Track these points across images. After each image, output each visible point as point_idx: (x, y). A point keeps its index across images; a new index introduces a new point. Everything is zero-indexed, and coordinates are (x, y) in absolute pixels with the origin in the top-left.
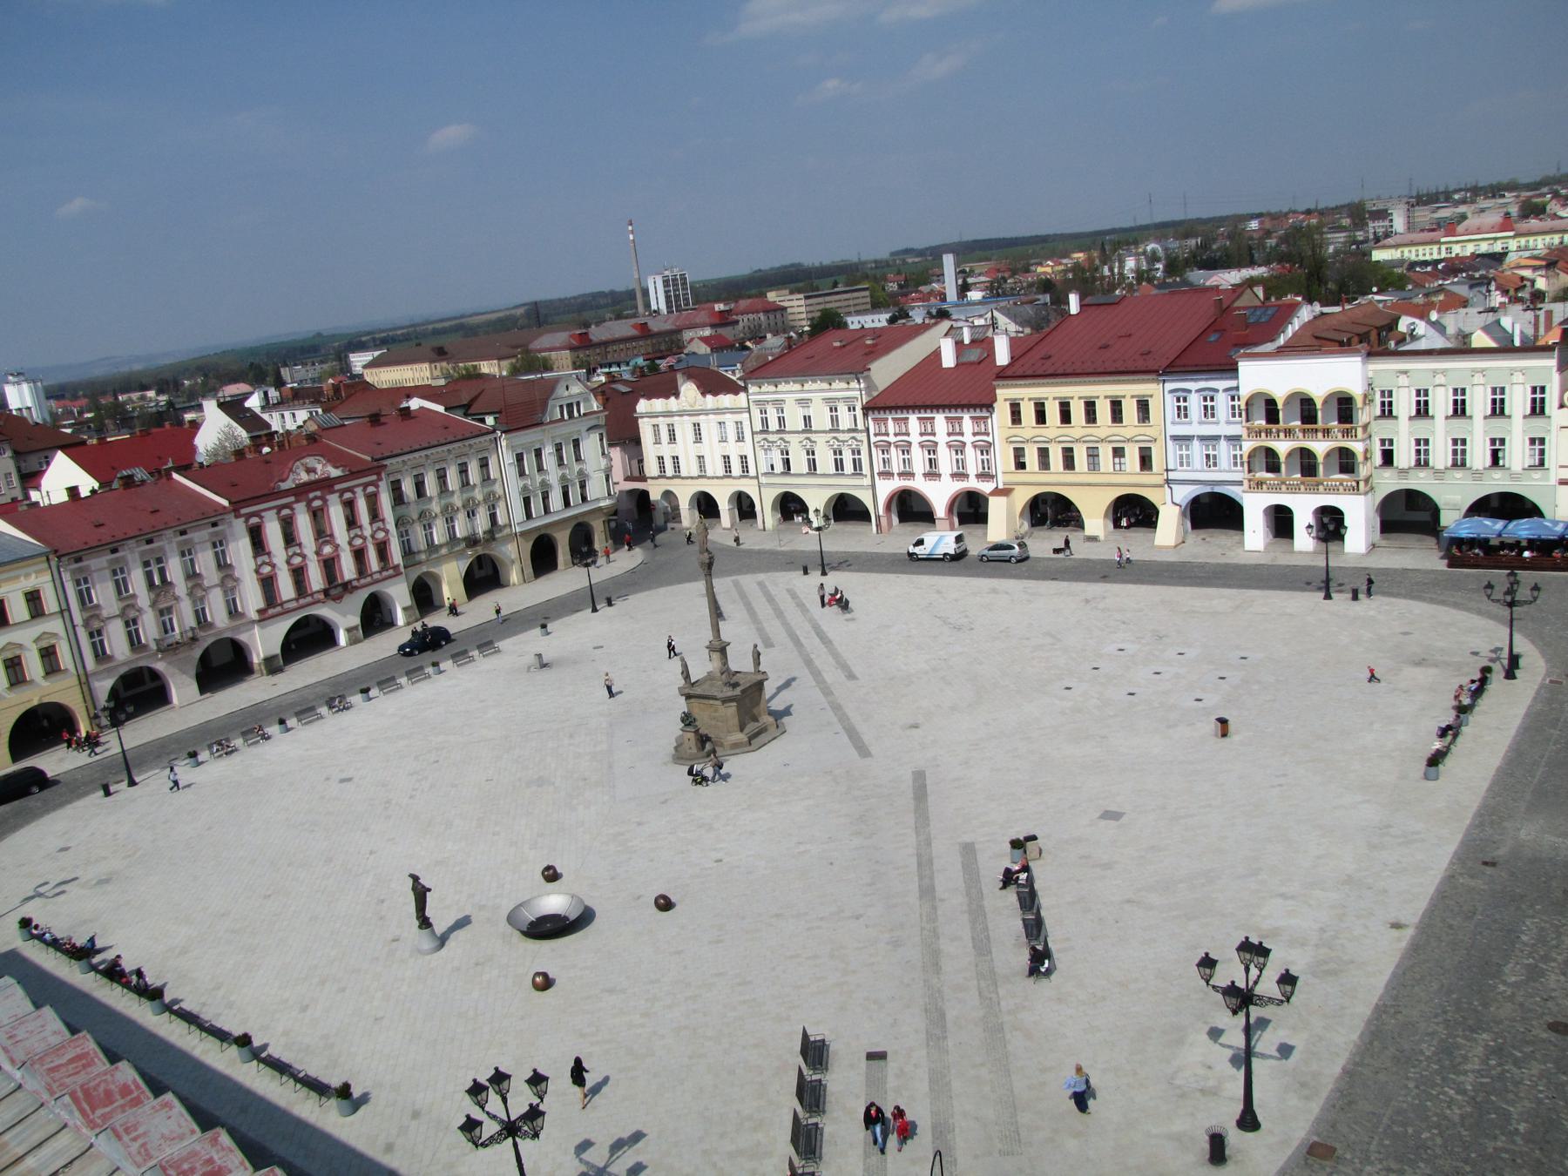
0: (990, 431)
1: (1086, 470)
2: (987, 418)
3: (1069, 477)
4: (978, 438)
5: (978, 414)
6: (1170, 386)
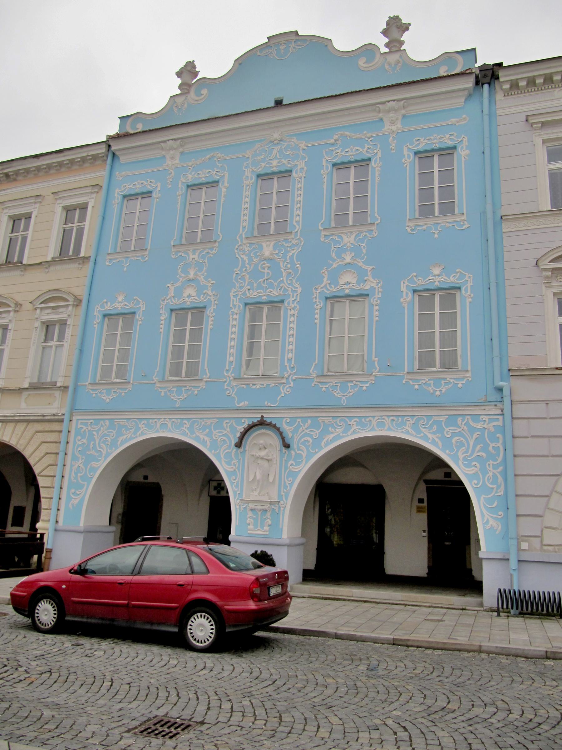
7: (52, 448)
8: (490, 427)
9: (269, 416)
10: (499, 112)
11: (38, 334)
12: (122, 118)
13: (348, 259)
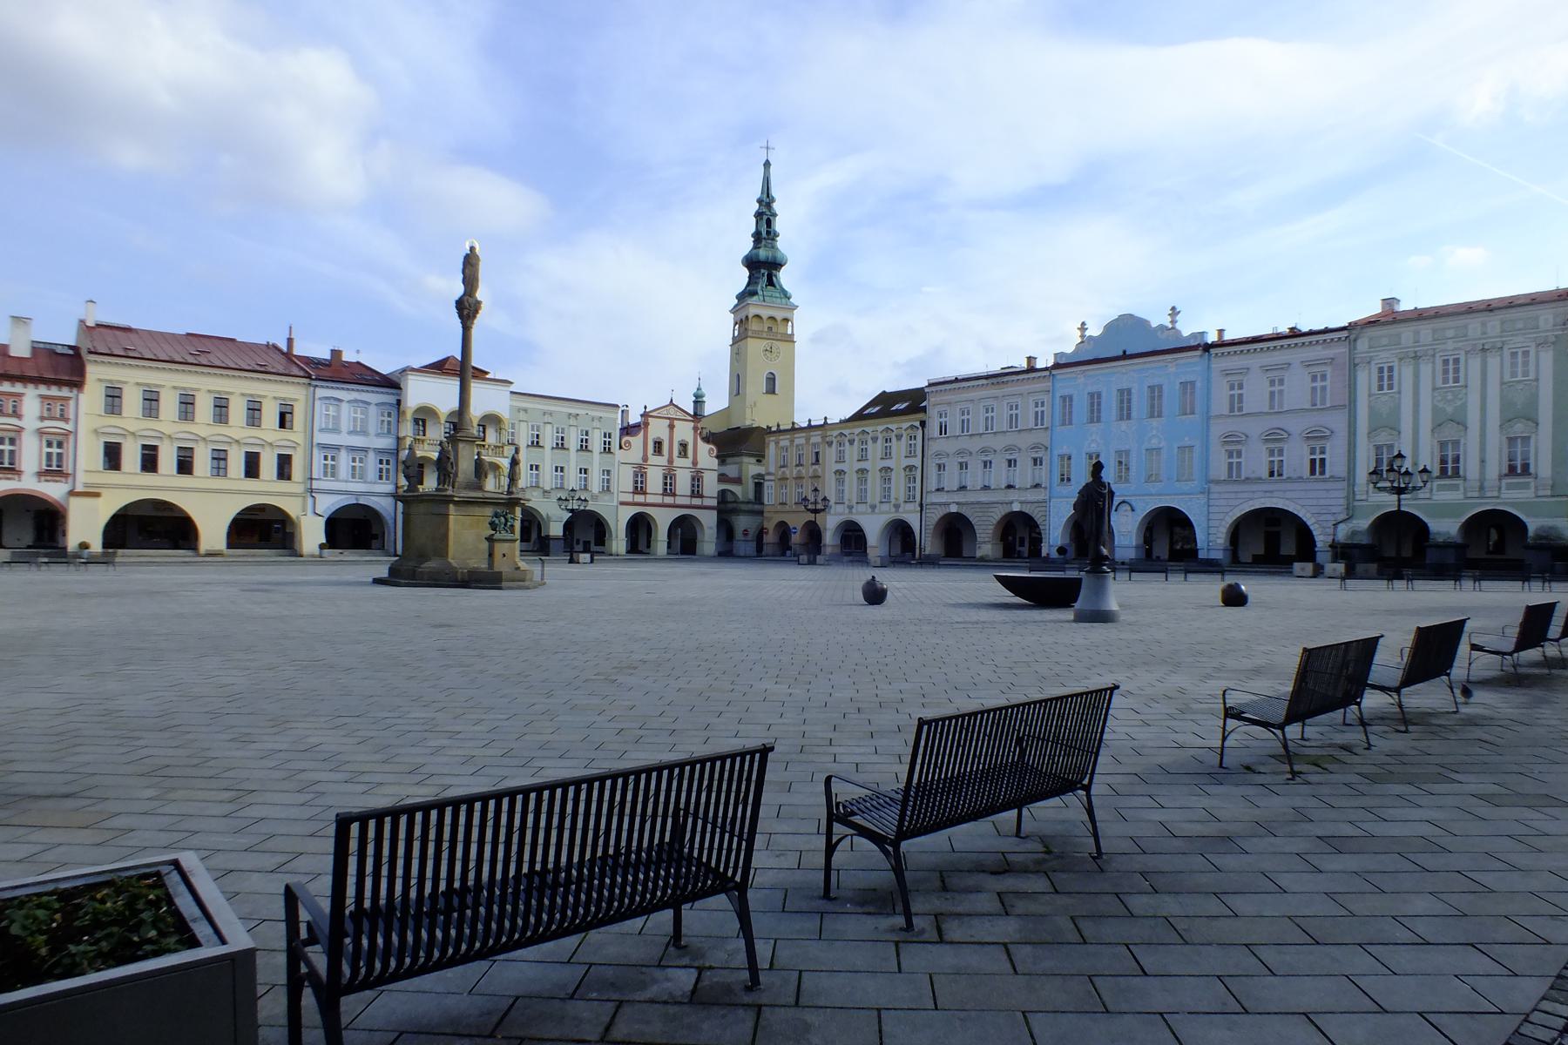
0: (72, 416)
1: (209, 475)
2: (68, 399)
3: (184, 480)
4: (47, 423)
5: (54, 391)
6: (320, 392)
7: (1043, 514)
8: (1202, 502)
9: (1126, 499)
10: (1213, 366)
11: (1031, 463)
12: (1056, 354)
13: (1154, 432)
